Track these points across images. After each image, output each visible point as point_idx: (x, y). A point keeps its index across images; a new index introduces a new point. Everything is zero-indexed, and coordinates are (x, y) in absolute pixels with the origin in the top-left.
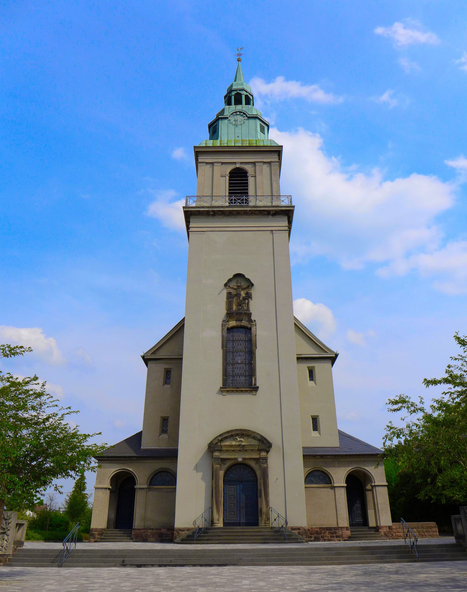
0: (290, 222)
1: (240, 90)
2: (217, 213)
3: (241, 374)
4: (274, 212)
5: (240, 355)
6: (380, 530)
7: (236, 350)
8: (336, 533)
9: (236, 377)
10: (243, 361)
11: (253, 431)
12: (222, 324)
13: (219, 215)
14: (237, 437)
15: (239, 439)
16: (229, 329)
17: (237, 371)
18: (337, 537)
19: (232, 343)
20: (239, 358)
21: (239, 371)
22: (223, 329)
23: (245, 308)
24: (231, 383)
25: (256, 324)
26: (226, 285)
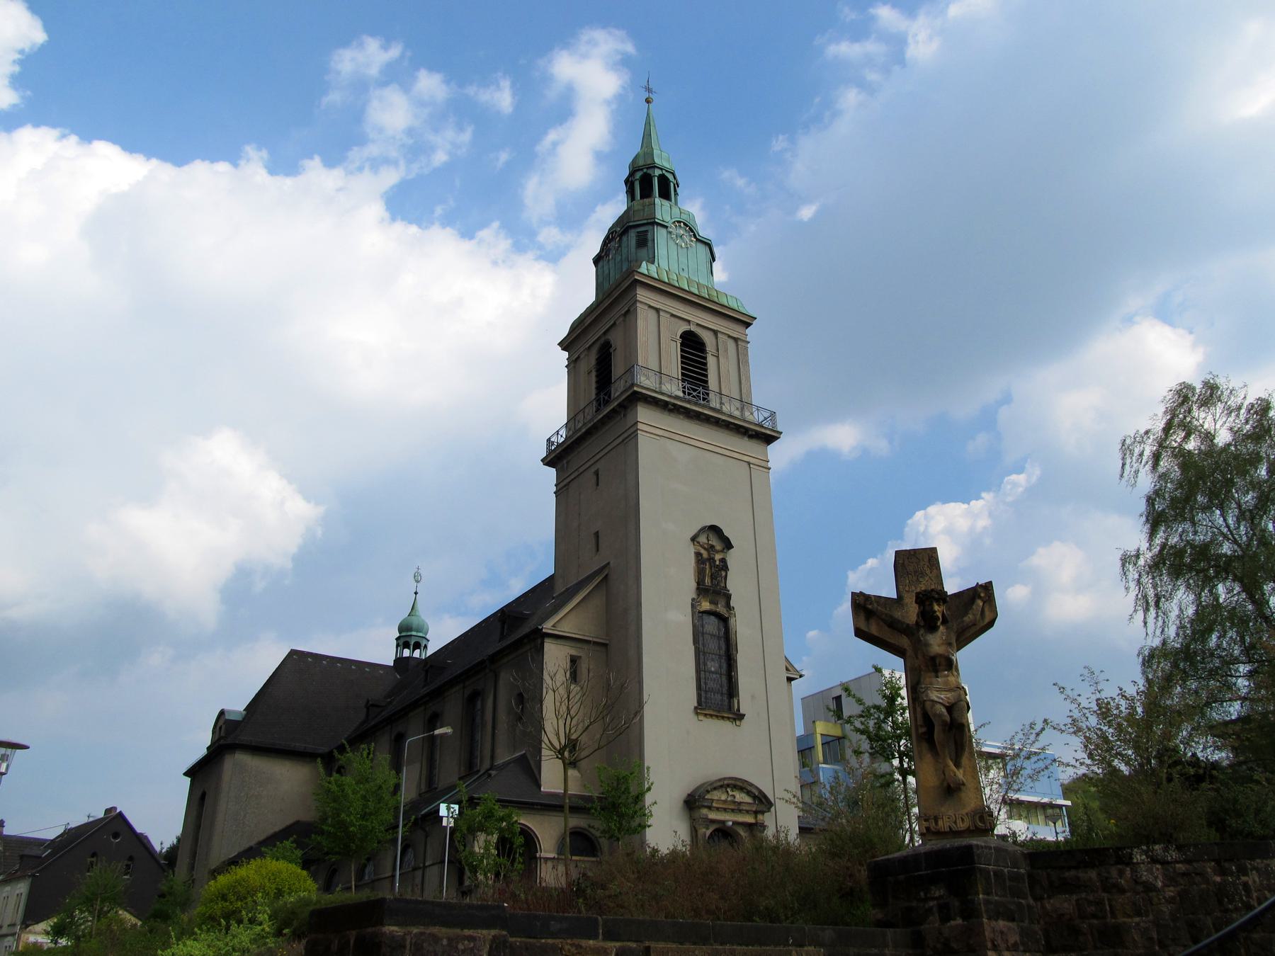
1: (666, 171)
4: (754, 433)
5: (713, 660)
9: (709, 693)
17: (711, 684)
26: (693, 539)
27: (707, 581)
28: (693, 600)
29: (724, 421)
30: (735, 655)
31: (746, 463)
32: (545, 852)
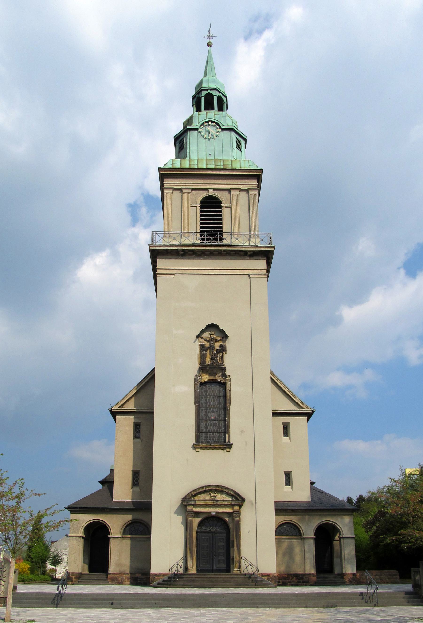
0: (269, 264)
1: (211, 89)
2: (188, 253)
3: (214, 430)
4: (252, 253)
5: (213, 412)
6: (344, 577)
7: (209, 406)
8: (303, 578)
9: (209, 433)
10: (216, 417)
11: (227, 487)
12: (195, 379)
13: (190, 255)
14: (211, 492)
15: (212, 495)
16: (202, 384)
17: (210, 428)
18: (304, 582)
19: (205, 399)
20: (213, 414)
21: (213, 427)
22: (195, 384)
23: (219, 361)
24: (205, 440)
25: (230, 379)
26: (198, 336)
27: (208, 361)
28: (196, 376)
29: (224, 250)
30: (228, 406)
31: (247, 275)
32: (114, 534)
